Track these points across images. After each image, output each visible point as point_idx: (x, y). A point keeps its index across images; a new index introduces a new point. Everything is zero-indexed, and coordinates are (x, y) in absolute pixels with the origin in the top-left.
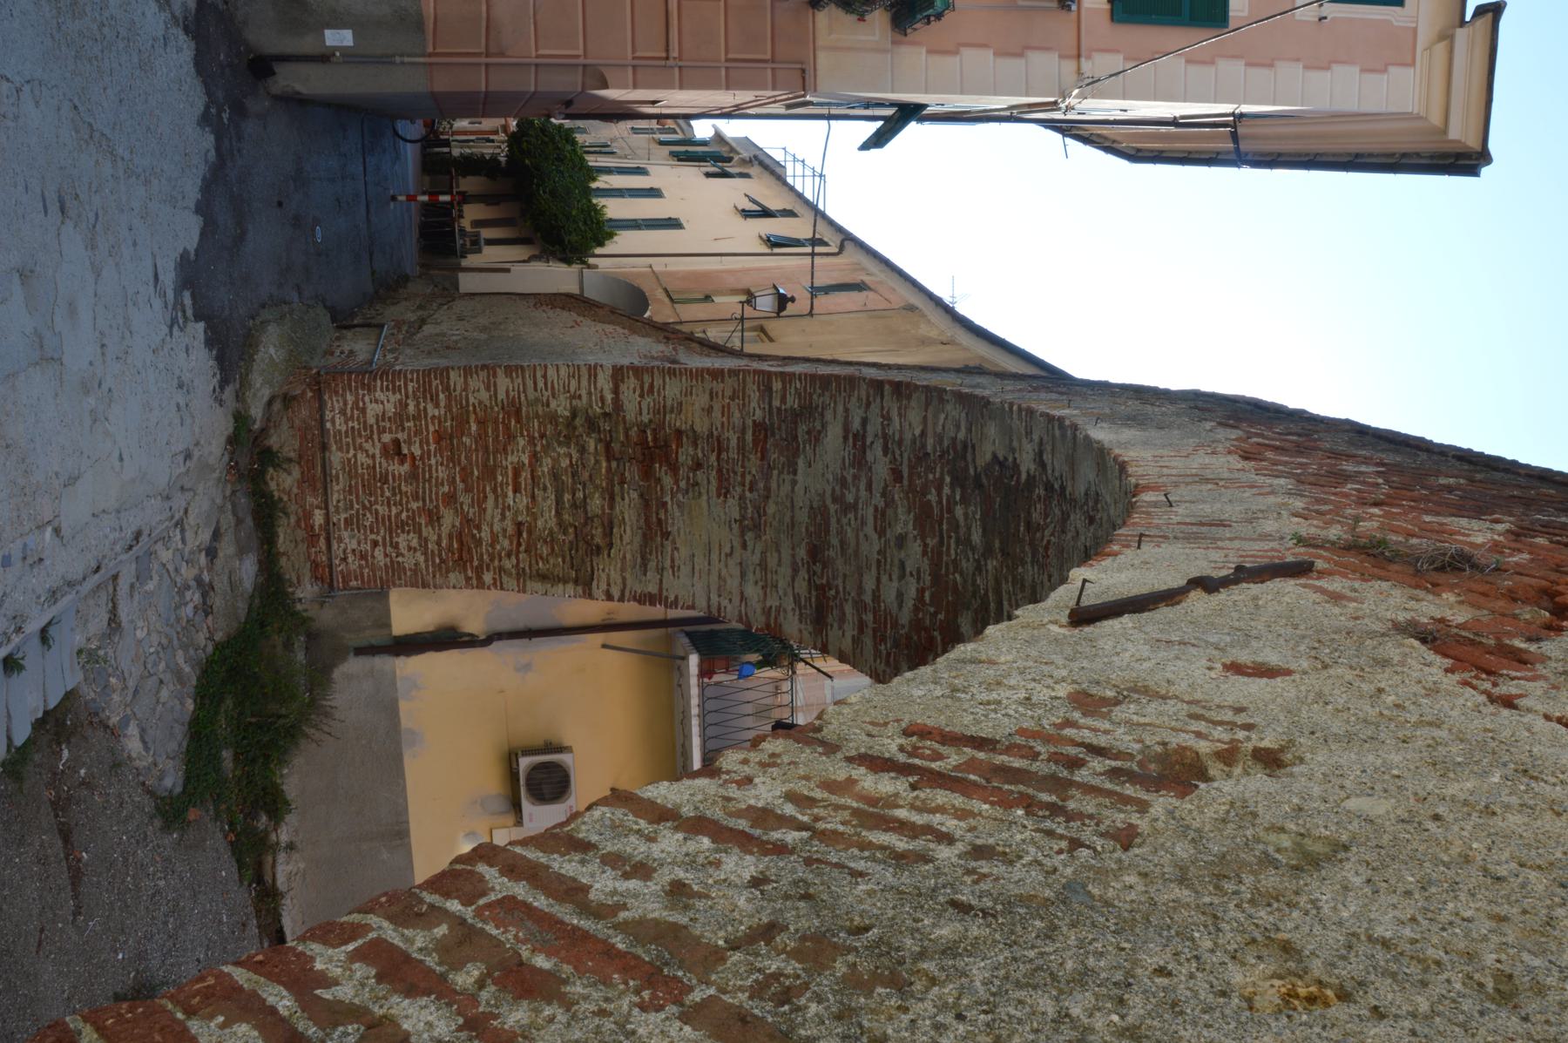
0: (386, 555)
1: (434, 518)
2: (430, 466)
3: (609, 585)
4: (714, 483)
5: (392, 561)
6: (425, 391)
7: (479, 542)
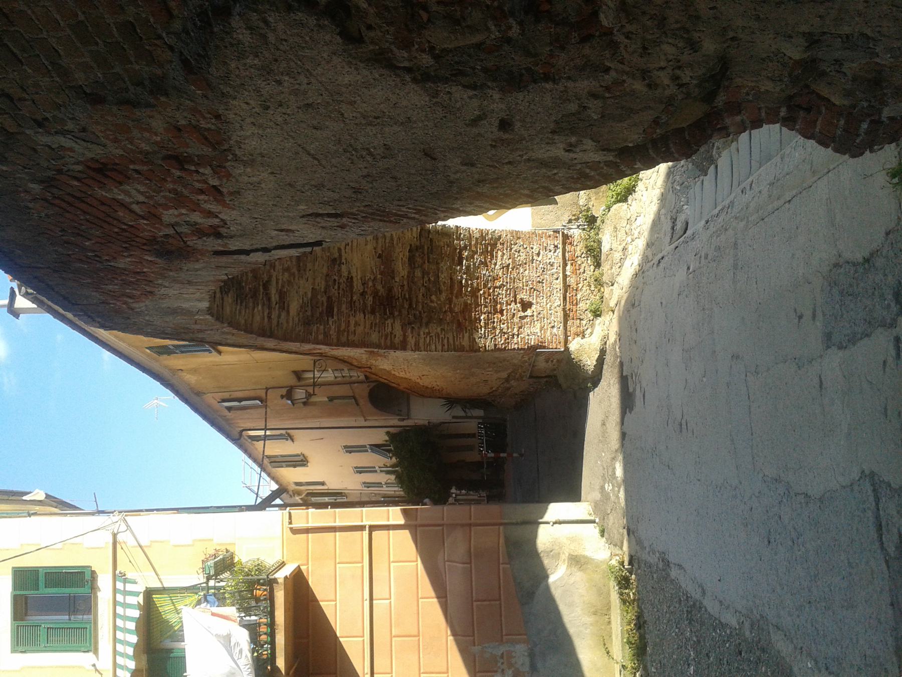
4: (355, 284)
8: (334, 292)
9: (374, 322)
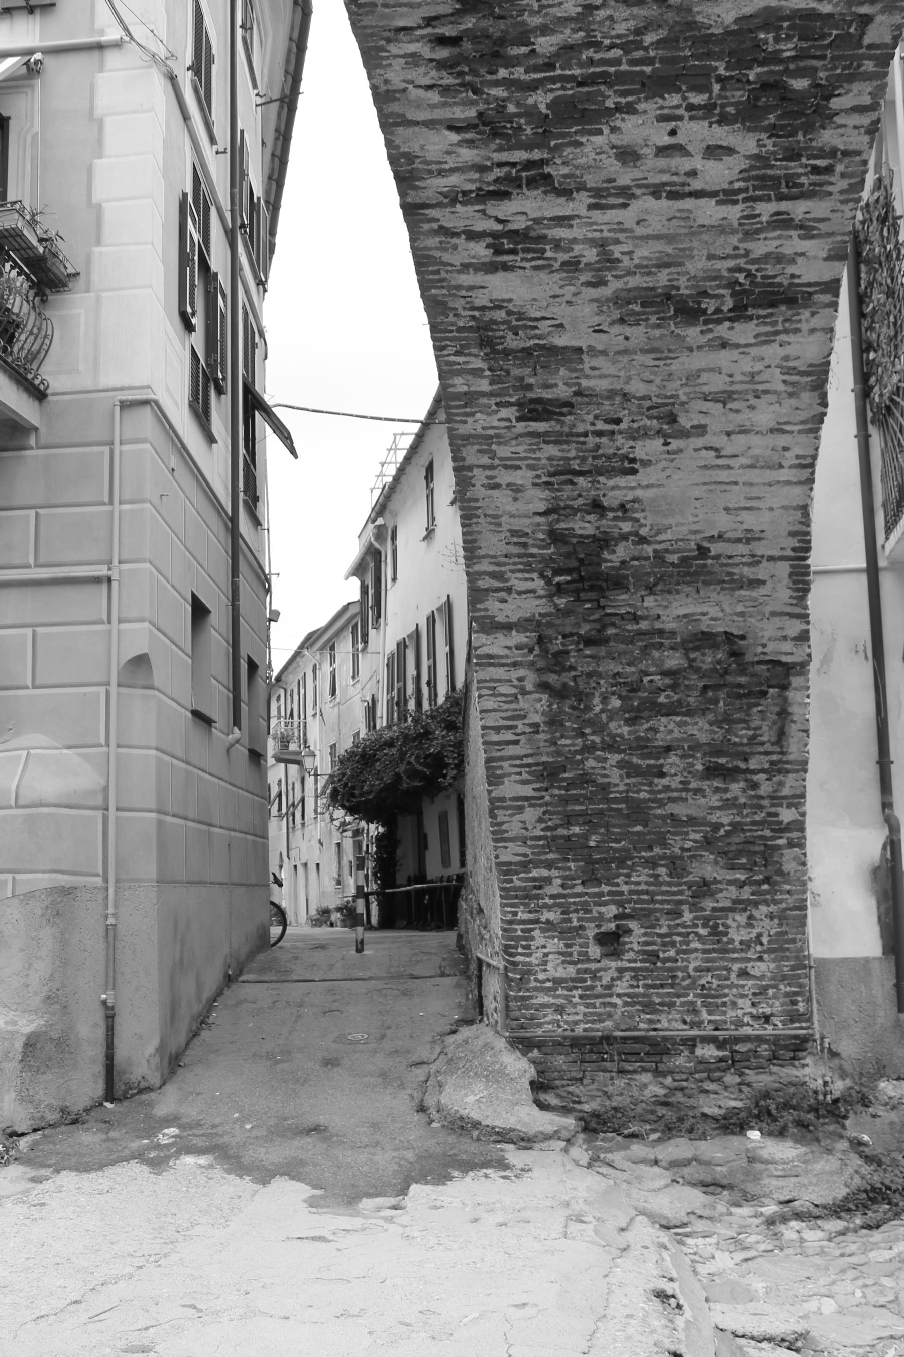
0: (760, 959)
1: (705, 888)
2: (631, 892)
3: (785, 638)
4: (621, 481)
5: (769, 951)
6: (526, 897)
7: (736, 827)
9: (530, 542)
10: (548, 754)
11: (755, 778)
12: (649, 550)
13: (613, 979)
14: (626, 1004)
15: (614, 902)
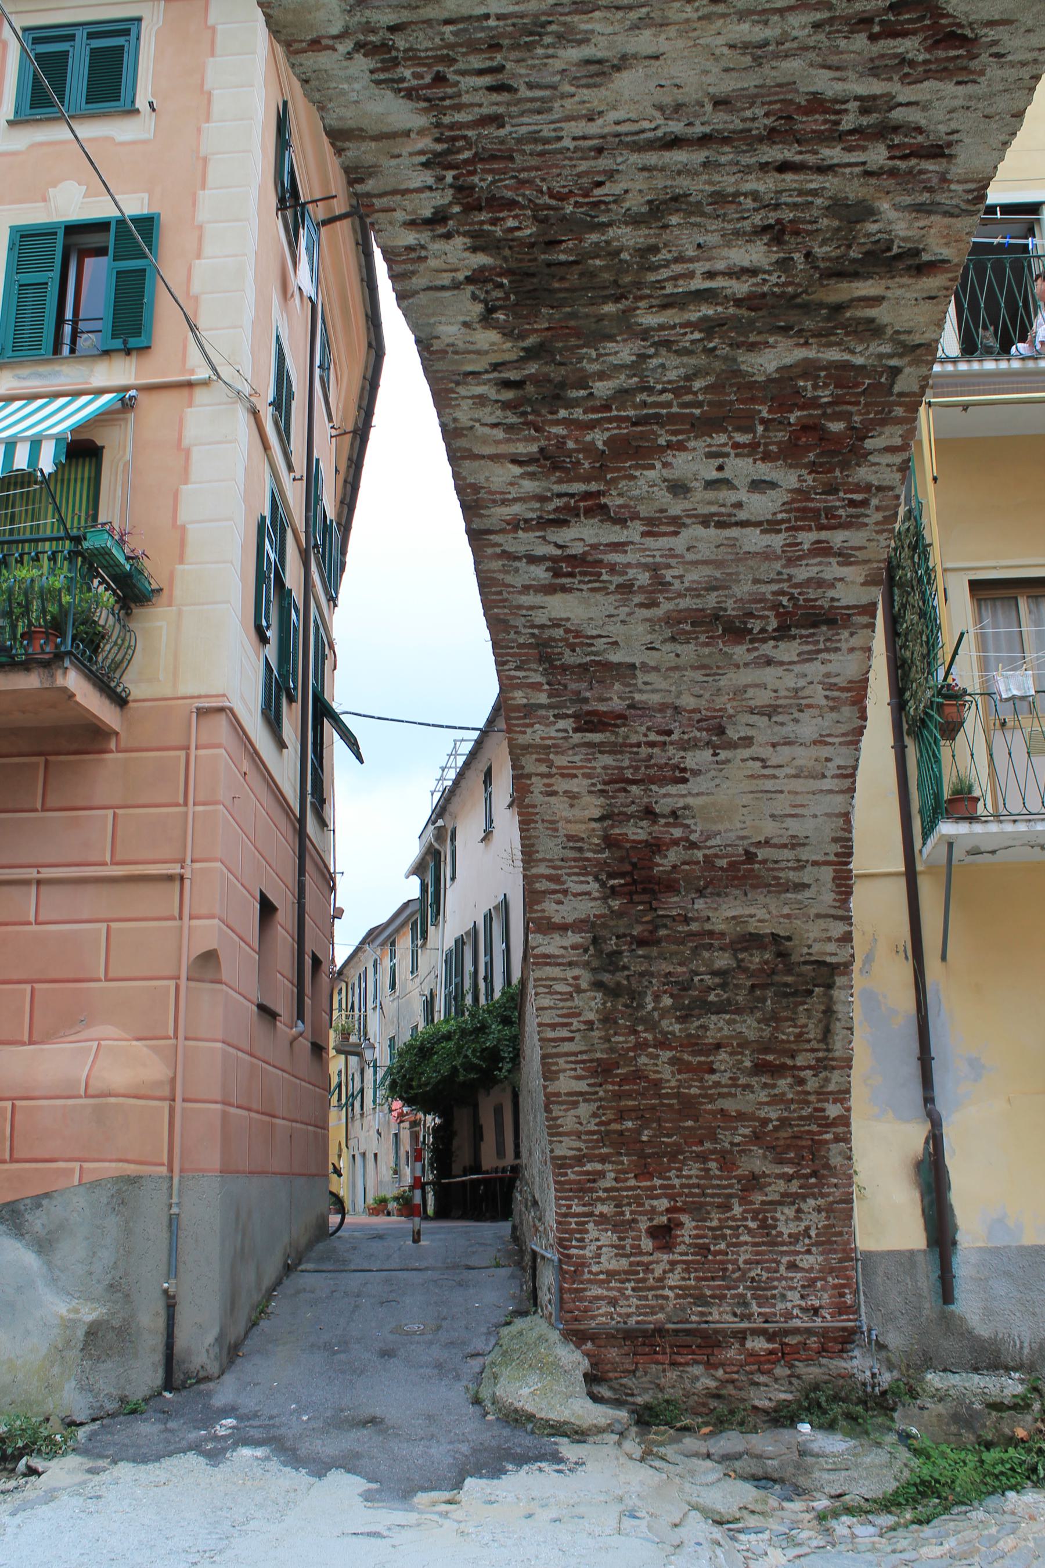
0: (809, 1252)
1: (754, 1182)
2: (683, 1186)
3: (829, 939)
4: (672, 789)
5: (817, 1244)
6: (581, 1190)
7: (784, 1122)
8: (637, 732)
9: (586, 846)
10: (602, 1051)
11: (802, 1074)
12: (699, 855)
13: (665, 1272)
14: (678, 1296)
15: (666, 1196)
